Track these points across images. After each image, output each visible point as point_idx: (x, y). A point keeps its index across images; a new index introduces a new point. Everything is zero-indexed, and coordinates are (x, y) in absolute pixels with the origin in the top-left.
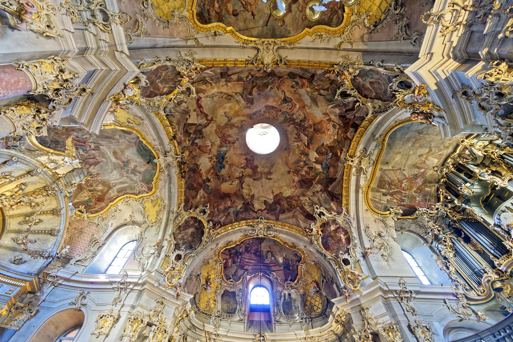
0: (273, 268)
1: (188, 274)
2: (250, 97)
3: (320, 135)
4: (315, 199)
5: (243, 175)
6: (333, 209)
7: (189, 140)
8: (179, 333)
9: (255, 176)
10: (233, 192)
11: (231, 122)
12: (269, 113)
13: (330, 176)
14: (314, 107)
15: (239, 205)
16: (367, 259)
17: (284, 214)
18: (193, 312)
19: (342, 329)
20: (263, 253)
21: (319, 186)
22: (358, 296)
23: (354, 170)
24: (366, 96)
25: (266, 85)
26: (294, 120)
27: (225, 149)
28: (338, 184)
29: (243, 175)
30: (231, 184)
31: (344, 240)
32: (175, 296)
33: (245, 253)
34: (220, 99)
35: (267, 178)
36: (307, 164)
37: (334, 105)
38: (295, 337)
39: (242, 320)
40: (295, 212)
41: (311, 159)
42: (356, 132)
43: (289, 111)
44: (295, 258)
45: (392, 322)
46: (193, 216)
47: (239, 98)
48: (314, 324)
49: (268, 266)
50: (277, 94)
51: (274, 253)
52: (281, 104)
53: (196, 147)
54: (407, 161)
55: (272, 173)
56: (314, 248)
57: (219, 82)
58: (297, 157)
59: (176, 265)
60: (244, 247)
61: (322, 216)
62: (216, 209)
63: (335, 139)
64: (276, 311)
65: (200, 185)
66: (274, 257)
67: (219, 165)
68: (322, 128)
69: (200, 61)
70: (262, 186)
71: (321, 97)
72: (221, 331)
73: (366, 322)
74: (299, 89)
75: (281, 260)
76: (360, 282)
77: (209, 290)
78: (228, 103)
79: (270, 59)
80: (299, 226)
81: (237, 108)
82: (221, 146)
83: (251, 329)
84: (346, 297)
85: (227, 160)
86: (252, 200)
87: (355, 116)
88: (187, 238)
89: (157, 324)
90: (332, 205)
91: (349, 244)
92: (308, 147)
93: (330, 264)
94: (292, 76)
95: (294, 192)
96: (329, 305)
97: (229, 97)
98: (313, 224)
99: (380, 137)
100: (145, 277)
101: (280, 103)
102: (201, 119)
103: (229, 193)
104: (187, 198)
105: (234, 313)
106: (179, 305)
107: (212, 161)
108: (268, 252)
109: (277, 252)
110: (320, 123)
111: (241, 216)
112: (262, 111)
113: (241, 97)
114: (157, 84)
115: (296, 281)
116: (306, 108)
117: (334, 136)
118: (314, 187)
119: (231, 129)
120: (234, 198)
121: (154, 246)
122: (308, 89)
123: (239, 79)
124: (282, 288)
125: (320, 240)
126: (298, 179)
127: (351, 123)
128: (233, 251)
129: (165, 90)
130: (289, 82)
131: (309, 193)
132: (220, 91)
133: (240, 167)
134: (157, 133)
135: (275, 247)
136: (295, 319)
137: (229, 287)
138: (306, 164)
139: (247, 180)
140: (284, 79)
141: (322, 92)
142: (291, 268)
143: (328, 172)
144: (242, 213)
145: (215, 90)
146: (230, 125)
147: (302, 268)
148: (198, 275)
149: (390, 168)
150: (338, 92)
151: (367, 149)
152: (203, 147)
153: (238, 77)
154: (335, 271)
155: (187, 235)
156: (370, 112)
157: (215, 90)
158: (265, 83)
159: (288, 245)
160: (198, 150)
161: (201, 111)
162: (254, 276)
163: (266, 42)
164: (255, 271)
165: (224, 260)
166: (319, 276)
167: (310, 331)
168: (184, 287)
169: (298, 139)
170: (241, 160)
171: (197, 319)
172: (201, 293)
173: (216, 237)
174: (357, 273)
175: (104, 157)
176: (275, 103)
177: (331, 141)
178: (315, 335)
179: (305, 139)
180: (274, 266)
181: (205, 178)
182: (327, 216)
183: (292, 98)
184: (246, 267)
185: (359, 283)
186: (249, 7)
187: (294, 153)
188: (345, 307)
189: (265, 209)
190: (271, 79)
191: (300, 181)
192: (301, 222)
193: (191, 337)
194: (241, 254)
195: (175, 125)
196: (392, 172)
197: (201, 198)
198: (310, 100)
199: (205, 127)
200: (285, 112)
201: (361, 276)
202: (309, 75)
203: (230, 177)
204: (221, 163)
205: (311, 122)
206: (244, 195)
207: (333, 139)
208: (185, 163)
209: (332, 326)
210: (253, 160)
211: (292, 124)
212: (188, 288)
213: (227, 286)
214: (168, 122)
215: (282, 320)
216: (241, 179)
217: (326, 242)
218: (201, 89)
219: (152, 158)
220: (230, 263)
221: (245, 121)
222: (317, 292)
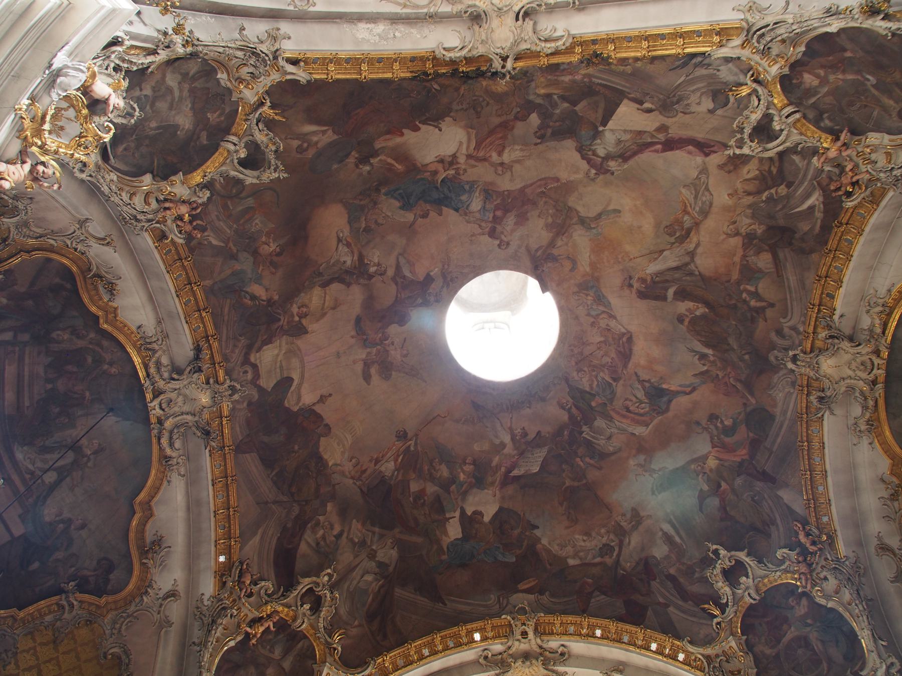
2: (671, 292)
4: (346, 557)
5: (371, 277)
7: (548, 96)
12: (605, 342)
15: (264, 288)
21: (394, 553)
24: (746, 629)
26: (588, 420)
27: (476, 204)
29: (371, 277)
30: (339, 240)
35: (367, 365)
36: (448, 492)
41: (470, 498)
42: (621, 619)
43: (618, 403)
47: (670, 259)
52: (641, 382)
57: (753, 216)
62: (250, 202)
70: (338, 355)
78: (657, 225)
79: (829, 371)
80: (244, 539)
81: (628, 248)
82: (488, 193)
85: (432, 214)
87: (667, 606)
94: (759, 420)
95: (343, 473)
98: (269, 585)
101: (644, 376)
102: (619, 142)
107: (440, 167)
112: (613, 323)
113: (672, 264)
114: (859, 72)
116: (642, 458)
117: (575, 556)
118: (382, 536)
119: (548, 227)
122: (712, 463)
125: (232, 644)
126: (388, 474)
130: (730, 409)
131: (357, 529)
132: (714, 209)
133: (402, 261)
139: (355, 296)
145: (721, 197)
150: (742, 555)
152: (504, 138)
153: (760, 271)
155: (171, 108)
156: (709, 651)
157: (721, 197)
159: (143, 524)
160: (496, 121)
163: (877, 361)
176: (643, 362)
177: (555, 549)
179: (533, 464)
181: (378, 145)
183: (670, 414)
189: (261, 390)
190: (742, 360)
191: (383, 480)
192: (257, 538)
197: (303, 137)
199: (580, 150)
200: (613, 393)
203: (363, 233)
205: (593, 475)
206: (303, 298)
207: (563, 553)
211: (571, 417)
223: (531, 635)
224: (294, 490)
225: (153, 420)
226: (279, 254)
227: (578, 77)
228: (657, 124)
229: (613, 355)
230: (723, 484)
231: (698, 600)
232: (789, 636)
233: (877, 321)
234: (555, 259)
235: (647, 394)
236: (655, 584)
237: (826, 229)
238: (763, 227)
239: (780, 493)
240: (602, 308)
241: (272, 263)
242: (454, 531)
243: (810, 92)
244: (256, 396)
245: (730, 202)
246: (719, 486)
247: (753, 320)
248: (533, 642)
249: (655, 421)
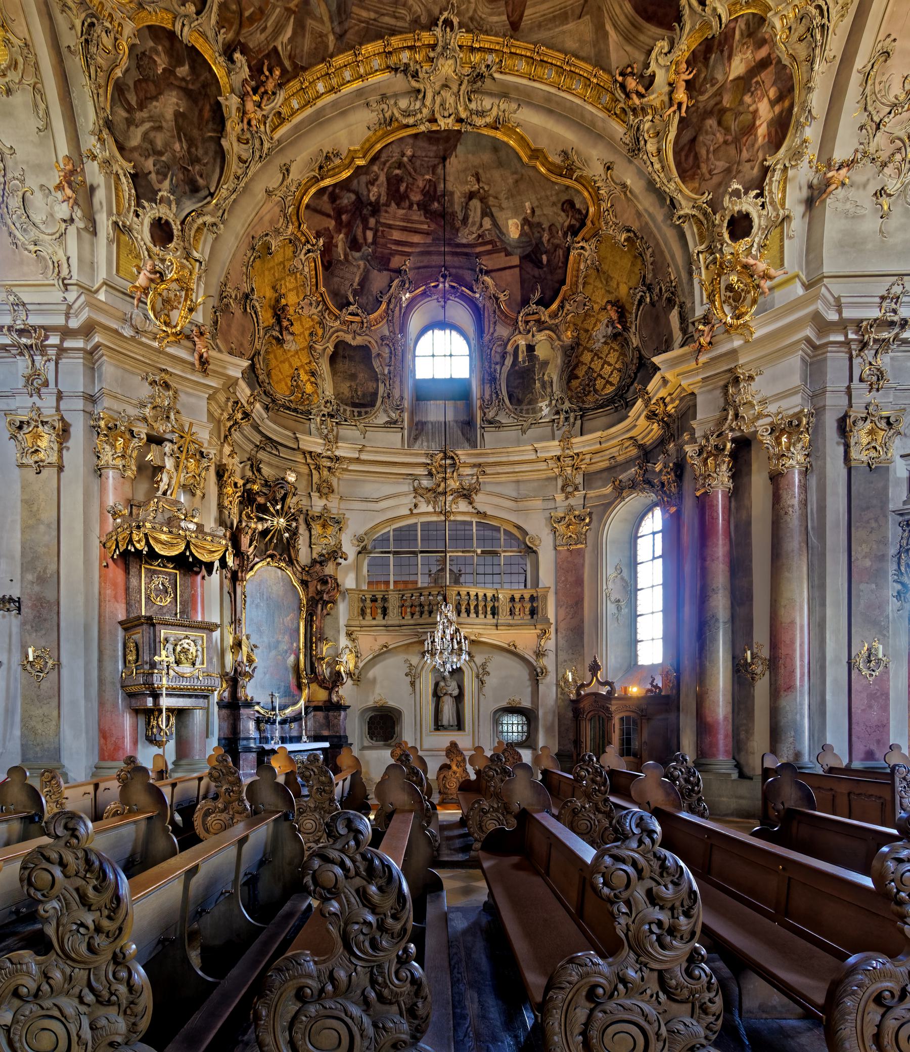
0: (487, 262)
1: (214, 291)
8: (237, 459)
16: (816, 212)
18: (258, 405)
19: (661, 432)
20: (451, 202)
22: (737, 343)
32: (197, 363)
33: (387, 205)
38: (534, 457)
39: (395, 422)
45: (802, 411)
48: (587, 425)
49: (466, 253)
51: (491, 201)
56: (640, 173)
59: (163, 261)
64: (487, 397)
66: (492, 216)
72: (343, 450)
73: (731, 413)
75: (513, 229)
76: (761, 300)
77: (291, 345)
83: (419, 442)
84: (700, 349)
89: (175, 437)
93: (682, 236)
96: (644, 370)
100: (81, 309)
105: (372, 404)
106: (217, 390)
108: (471, 196)
109: (502, 196)
115: (554, 306)
121: (59, 187)
124: (511, 329)
128: (347, 199)
135: (496, 174)
136: (539, 415)
137: (347, 332)
142: (544, 258)
147: (583, 253)
148: (246, 296)
154: (690, 263)
162: (424, 294)
164: (425, 279)
165: (318, 235)
166: (632, 284)
167: (574, 440)
168: (214, 337)
171: (275, 423)
172: (267, 352)
173: (277, 135)
174: (762, 266)
178: (584, 450)
180: (489, 253)
185: (754, 301)
188: (687, 378)
193: (269, 464)
194: (376, 209)
201: (771, 278)
209: (635, 426)
212: (226, 341)
213: (340, 328)
215: (504, 420)
222: (615, 336)
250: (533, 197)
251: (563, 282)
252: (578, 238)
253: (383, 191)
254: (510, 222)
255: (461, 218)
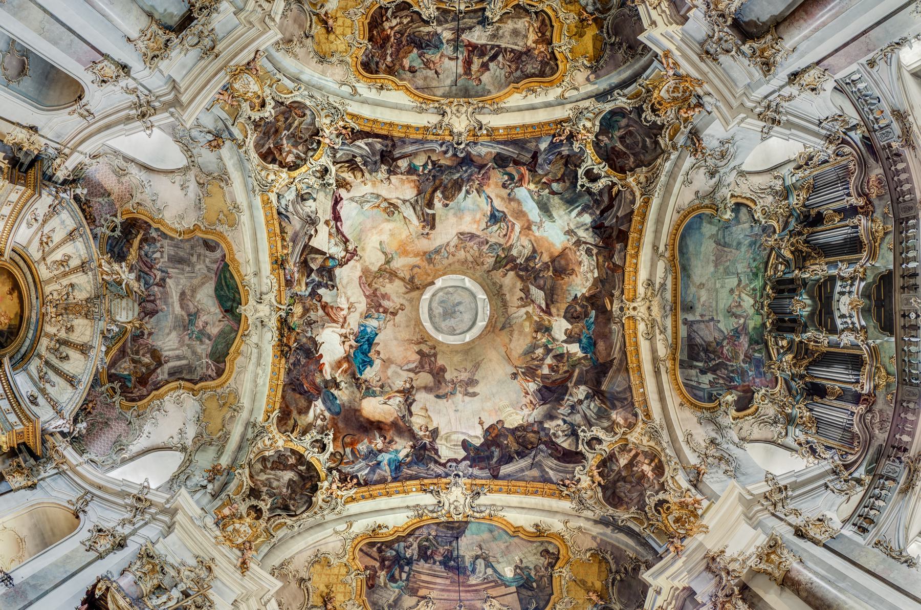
3: (566, 279)
4: (578, 418)
5: (412, 387)
6: (618, 424)
7: (307, 284)
9: (439, 388)
10: (389, 419)
11: (391, 264)
12: (464, 248)
13: (601, 361)
14: (547, 224)
15: (403, 448)
17: (511, 465)
20: (464, 562)
23: (641, 327)
25: (458, 186)
26: (513, 259)
27: (373, 323)
28: (619, 370)
30: (385, 403)
31: (650, 474)
34: (376, 210)
35: (466, 394)
37: (580, 208)
40: (535, 456)
41: (557, 336)
42: (626, 246)
43: (502, 241)
44: (543, 561)
46: (295, 448)
50: (478, 206)
51: (491, 559)
53: (319, 304)
54: (717, 302)
55: (477, 382)
58: (528, 340)
60: (415, 545)
61: (597, 447)
62: (348, 450)
63: (595, 279)
65: (318, 389)
66: (493, 567)
67: (361, 356)
68: (568, 265)
69: (353, 116)
71: (556, 197)
74: (516, 190)
80: (546, 480)
85: (378, 349)
86: (434, 440)
88: (278, 487)
90: (614, 416)
91: (662, 474)
92: (548, 312)
94: (501, 161)
95: (529, 415)
97: (391, 208)
98: (578, 468)
99: (666, 249)
101: (484, 226)
103: (379, 422)
104: (287, 407)
108: (477, 557)
109: (498, 556)
110: (563, 254)
111: (406, 471)
112: (452, 244)
114: (281, 139)
116: (534, 228)
117: (592, 271)
118: (571, 395)
119: (391, 281)
120: (390, 434)
122: (532, 186)
123: (412, 170)
125: (600, 495)
127: (615, 234)
128: (390, 553)
129: (290, 159)
130: (497, 177)
131: (563, 410)
132: (375, 192)
134: (256, 251)
135: (494, 545)
138: (548, 351)
139: (422, 398)
140: (489, 169)
141: (555, 186)
142: (534, 585)
143: (594, 353)
144: (409, 465)
145: (368, 189)
146: (387, 272)
149: (698, 318)
150: (580, 172)
151: (653, 279)
152: (332, 307)
153: (409, 165)
155: (279, 481)
157: (368, 189)
158: (456, 181)
160: (321, 312)
161: (337, 227)
163: (455, 103)
169: (527, 299)
170: (409, 353)
175: (166, 303)
176: (475, 226)
177: (589, 284)
179: (539, 295)
180: (493, 587)
182: (608, 443)
183: (506, 210)
184: (422, 592)
186: (432, 65)
187: (521, 332)
189: (464, 459)
190: (466, 171)
191: (539, 391)
194: (409, 562)
195: (288, 239)
196: (702, 326)
198: (538, 210)
200: (496, 244)
202: (526, 157)
204: (365, 354)
205: (546, 258)
206: (416, 428)
207: (591, 280)
208: (293, 329)
210: (435, 355)
211: (511, 269)
214: (277, 225)
216: (407, 394)
217: (614, 493)
218: (344, 180)
219: (235, 305)
220: (382, 579)
221: (419, 267)
223: (635, 305)
224: (530, 447)
225: (465, 520)
226: (385, 438)
227: (296, 269)
228: (325, 226)
229: (472, 243)
230: (544, 180)
231: (612, 199)
232: (621, 147)
233: (431, 106)
234: (412, 278)
235: (495, 224)
236: (607, 223)
237: (377, 136)
238: (383, 166)
239: (542, 149)
240: (443, 250)
241: (389, 443)
242: (575, 348)
243: (298, 157)
244: (468, 462)
245: (370, 184)
246: (545, 183)
247: (440, 166)
248: (640, 304)
249: (511, 219)
250: (520, 554)
251: (552, 594)
252: (556, 568)
253: (416, 553)
254: (506, 569)
255: (470, 569)
